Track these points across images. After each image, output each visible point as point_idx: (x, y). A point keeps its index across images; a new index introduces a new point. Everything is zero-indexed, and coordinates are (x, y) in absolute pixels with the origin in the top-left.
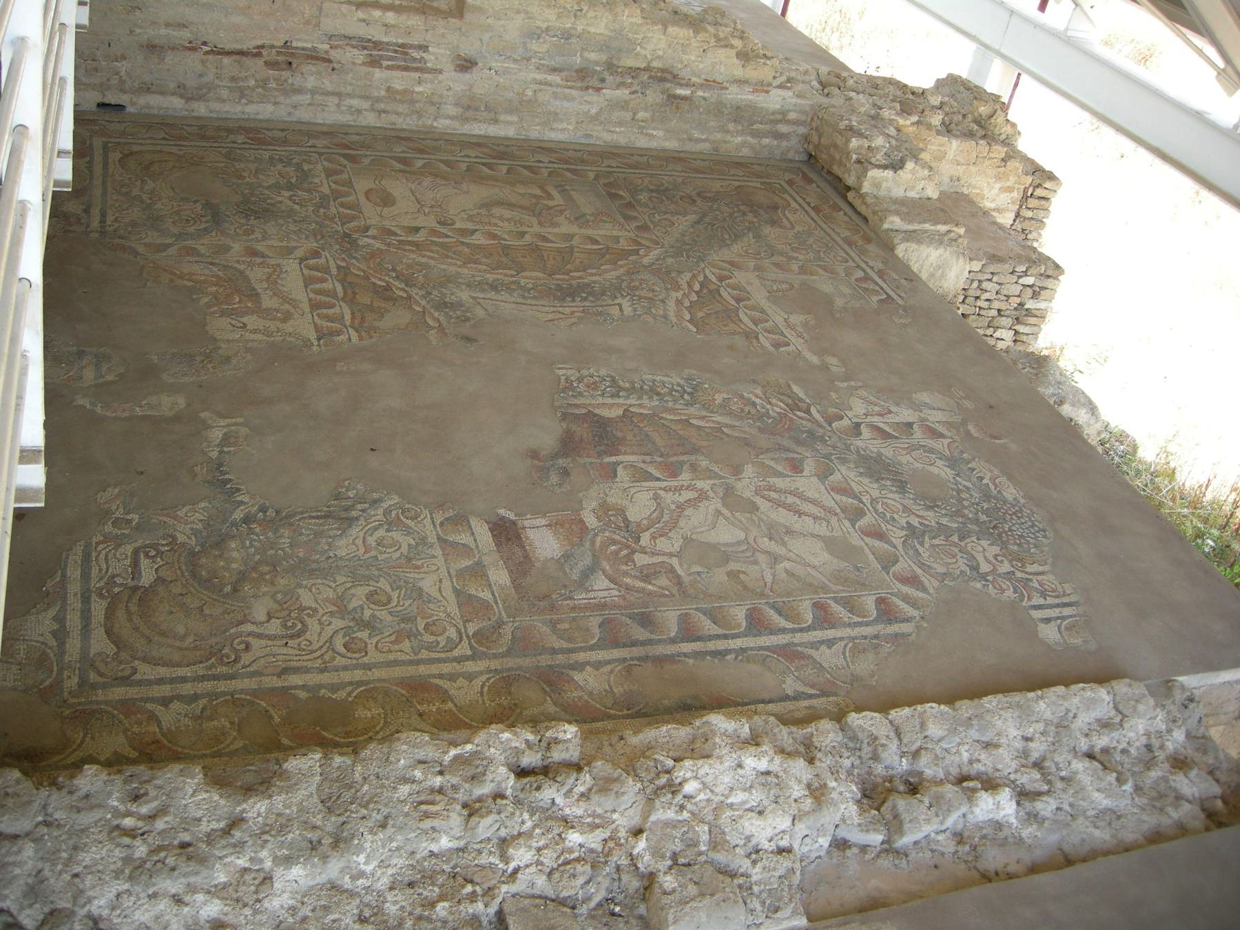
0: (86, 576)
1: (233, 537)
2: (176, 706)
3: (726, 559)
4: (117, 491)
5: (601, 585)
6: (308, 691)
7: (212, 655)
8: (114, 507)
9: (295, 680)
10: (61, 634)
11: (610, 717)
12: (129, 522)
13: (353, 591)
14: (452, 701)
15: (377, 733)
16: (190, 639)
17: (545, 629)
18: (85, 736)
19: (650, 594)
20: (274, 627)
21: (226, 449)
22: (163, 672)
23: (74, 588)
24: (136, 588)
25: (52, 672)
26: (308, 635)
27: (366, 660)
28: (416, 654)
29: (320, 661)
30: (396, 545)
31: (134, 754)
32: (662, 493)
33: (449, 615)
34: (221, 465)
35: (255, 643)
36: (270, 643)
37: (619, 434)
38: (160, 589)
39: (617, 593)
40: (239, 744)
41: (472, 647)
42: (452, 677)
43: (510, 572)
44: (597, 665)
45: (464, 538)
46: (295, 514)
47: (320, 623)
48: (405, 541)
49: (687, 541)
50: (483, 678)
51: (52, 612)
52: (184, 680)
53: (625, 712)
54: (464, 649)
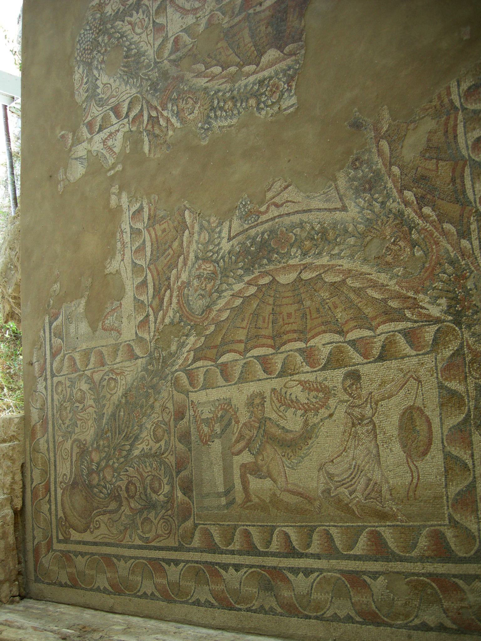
37: (270, 29)
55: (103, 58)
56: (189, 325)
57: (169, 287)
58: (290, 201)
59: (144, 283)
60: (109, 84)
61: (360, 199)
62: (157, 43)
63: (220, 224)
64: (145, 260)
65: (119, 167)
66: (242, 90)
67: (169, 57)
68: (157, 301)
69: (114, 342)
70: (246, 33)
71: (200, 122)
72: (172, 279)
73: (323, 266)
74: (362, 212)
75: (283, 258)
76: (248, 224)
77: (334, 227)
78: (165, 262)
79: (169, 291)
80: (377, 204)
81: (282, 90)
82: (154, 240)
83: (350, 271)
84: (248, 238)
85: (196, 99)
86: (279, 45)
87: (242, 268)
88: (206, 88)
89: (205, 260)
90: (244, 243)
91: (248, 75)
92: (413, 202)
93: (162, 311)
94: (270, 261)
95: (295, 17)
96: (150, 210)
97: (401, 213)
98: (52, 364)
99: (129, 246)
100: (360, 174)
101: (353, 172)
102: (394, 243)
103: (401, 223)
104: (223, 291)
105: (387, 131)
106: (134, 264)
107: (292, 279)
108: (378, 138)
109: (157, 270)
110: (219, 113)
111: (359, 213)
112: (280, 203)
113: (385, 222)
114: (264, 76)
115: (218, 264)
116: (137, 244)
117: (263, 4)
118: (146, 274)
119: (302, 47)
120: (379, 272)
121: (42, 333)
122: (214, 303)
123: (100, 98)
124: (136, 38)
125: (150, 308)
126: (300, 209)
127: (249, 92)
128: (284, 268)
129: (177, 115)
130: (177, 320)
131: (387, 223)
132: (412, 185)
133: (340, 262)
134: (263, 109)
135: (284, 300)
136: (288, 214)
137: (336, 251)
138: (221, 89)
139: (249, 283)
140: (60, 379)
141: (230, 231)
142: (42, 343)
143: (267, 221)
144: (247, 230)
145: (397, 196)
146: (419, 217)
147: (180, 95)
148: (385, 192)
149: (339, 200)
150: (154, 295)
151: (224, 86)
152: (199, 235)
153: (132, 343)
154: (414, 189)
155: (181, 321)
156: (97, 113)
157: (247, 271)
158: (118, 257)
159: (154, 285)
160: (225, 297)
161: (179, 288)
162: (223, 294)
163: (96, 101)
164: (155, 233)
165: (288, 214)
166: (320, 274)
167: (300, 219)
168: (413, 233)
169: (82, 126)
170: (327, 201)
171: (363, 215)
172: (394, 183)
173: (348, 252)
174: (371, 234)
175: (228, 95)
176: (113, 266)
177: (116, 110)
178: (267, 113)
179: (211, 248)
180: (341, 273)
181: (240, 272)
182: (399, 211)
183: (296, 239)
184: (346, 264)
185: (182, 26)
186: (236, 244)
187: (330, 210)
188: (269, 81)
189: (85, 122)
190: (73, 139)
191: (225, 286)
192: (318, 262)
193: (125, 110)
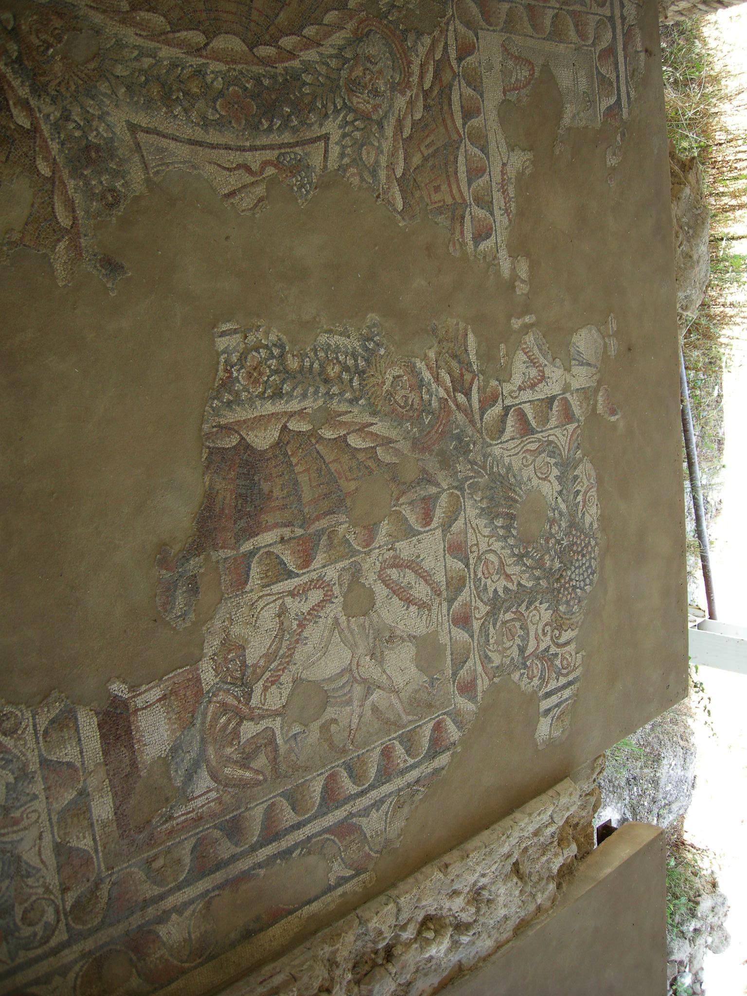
5: (204, 782)
11: (183, 972)
17: (140, 875)
32: (288, 600)
33: (47, 890)
37: (265, 487)
39: (213, 795)
43: (115, 795)
45: (68, 753)
53: (198, 961)
55: (551, 528)
56: (390, 22)
57: (426, 94)
58: (224, 168)
59: (468, 115)
60: (539, 478)
61: (105, 135)
62: (459, 524)
63: (343, 168)
64: (466, 151)
65: (516, 324)
66: (311, 390)
67: (439, 493)
68: (447, 76)
69: (512, 36)
70: (307, 495)
71: (382, 357)
72: (420, 104)
73: (168, 43)
74: (103, 113)
75: (236, 77)
76: (295, 154)
77: (150, 102)
78: (432, 137)
79: (427, 86)
80: (77, 119)
81: (241, 368)
82: (452, 179)
83: (123, 22)
84: (294, 130)
85: (390, 401)
86: (249, 452)
87: (305, 84)
88: (374, 414)
89: (366, 117)
90: (302, 123)
91: (301, 413)
92: (14, 104)
93: (437, 59)
94: (258, 80)
95: (220, 497)
96: (462, 233)
97: (38, 90)
98: (614, 38)
99: (494, 184)
100: (104, 178)
101: (118, 185)
102: (49, 46)
103: (35, 75)
104: (336, 56)
105: (59, 240)
106: (484, 149)
107: (221, 38)
108: (73, 232)
109: (446, 126)
110: (350, 362)
111: (108, 114)
112: (241, 171)
113: (63, 84)
114: (273, 404)
115: (345, 103)
116: (481, 181)
117: (278, 540)
118: (464, 128)
119: (208, 436)
120: (73, 5)
121: (633, 94)
122: (349, 43)
123: (554, 457)
124: (497, 546)
125: (456, 70)
126: (207, 150)
127: (299, 383)
128: (234, 62)
129: (421, 384)
130: (411, 37)
131: (60, 83)
132: (17, 136)
133: (140, 41)
134: (275, 345)
135: (234, 10)
136: (227, 148)
137: (147, 62)
138: (346, 404)
139: (292, 55)
140: (600, 11)
141: (326, 151)
142: (632, 78)
143: (264, 148)
144: (297, 144)
145: (42, 122)
146: (5, 77)
147: (418, 416)
148: (62, 136)
149: (141, 144)
150: (451, 90)
151: (343, 407)
152: (377, 162)
153: (483, 24)
154: (13, 127)
155: (405, 32)
156: (558, 432)
157: (295, 76)
158: (511, 172)
159: (450, 105)
160: (331, 46)
161: (408, 85)
162: (336, 52)
163: (560, 455)
164: (451, 191)
165: (227, 148)
166: (173, 32)
167: (208, 134)
168: (16, 54)
169: (582, 419)
170: (161, 150)
171: (100, 108)
172: (47, 147)
173: (125, 52)
174: (86, 71)
175: (335, 390)
176: (518, 161)
177: (526, 429)
178: (267, 334)
179: (357, 134)
180: (138, 24)
181: (308, 79)
182: (39, 96)
183: (215, 103)
184: (130, 36)
185: (419, 541)
186: (316, 126)
187: (158, 133)
188: (264, 392)
189: (576, 425)
190: (596, 401)
191: (333, 63)
192: (177, 53)
193: (510, 421)
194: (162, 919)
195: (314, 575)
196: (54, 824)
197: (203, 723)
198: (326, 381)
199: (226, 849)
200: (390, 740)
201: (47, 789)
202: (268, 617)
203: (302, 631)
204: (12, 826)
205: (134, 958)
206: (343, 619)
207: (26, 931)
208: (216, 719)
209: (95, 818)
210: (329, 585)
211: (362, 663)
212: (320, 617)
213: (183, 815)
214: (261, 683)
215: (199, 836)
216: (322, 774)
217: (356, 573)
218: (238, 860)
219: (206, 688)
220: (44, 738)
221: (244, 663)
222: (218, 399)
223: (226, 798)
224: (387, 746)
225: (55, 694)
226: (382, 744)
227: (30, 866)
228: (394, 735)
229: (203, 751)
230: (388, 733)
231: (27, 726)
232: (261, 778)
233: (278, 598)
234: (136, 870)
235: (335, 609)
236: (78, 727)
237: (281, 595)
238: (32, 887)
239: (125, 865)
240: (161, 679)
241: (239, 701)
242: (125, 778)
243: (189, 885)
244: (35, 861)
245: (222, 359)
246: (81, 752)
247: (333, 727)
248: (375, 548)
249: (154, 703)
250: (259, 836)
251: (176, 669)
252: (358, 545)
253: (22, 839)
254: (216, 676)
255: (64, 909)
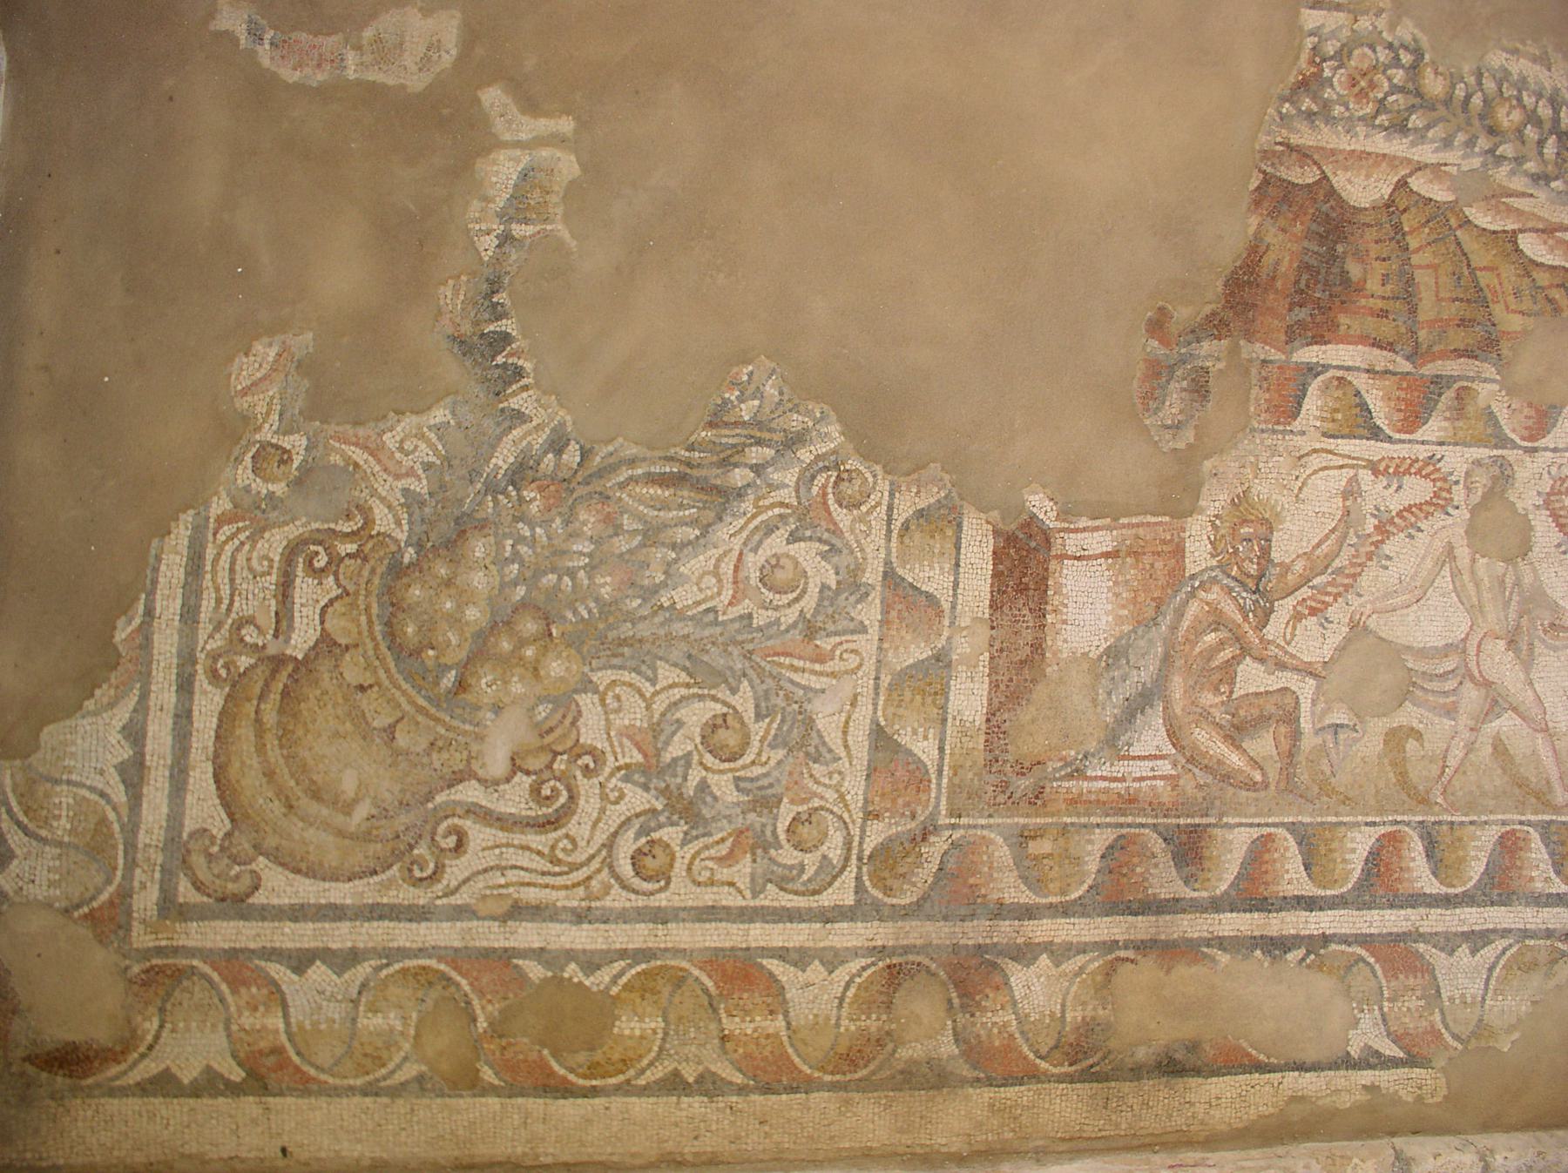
0: (189, 614)
1: (482, 526)
2: (319, 972)
3: (1405, 693)
4: (272, 353)
5: (1151, 736)
6: (548, 965)
7: (397, 855)
8: (261, 408)
9: (527, 935)
10: (134, 774)
11: (1034, 1076)
12: (285, 457)
13: (681, 713)
14: (786, 1014)
15: (643, 1071)
16: (362, 811)
17: (1003, 852)
18: (161, 1027)
19: (1227, 777)
20: (515, 799)
21: (518, 230)
22: (308, 891)
23: (166, 644)
24: (279, 661)
25: (115, 868)
26: (572, 827)
27: (661, 900)
28: (755, 895)
29: (581, 891)
30: (795, 586)
31: (237, 1075)
32: (1366, 476)
33: (842, 797)
34: (494, 286)
35: (480, 835)
36: (502, 836)
37: (1354, 270)
38: (324, 666)
39: (1165, 767)
40: (411, 1070)
41: (859, 888)
42: (799, 958)
43: (995, 686)
44: (1061, 952)
45: (932, 578)
46: (612, 469)
47: (604, 797)
48: (822, 574)
49: (1357, 628)
50: (855, 965)
51: (122, 714)
52: (336, 913)
53: (1066, 1069)
54: (842, 893)
81: (1340, 67)
86: (1332, 203)
91: (1437, 170)
114: (1388, 139)
134: (1406, 48)
138: (1525, 180)
151: (1518, 184)
175: (1506, 149)
178: (1392, 27)
194: (1024, 953)
195: (1423, 452)
196: (882, 691)
197: (1174, 628)
198: (1492, 131)
199: (1165, 881)
200: (1521, 823)
201: (885, 622)
202: (1326, 488)
203: (1382, 542)
204: (813, 661)
205: (956, 1001)
206: (1463, 553)
207: (788, 856)
208: (1197, 631)
209: (952, 708)
210: (1445, 480)
211: (1488, 646)
212: (1419, 530)
213: (1103, 778)
214: (1290, 602)
215: (1124, 831)
216: (1374, 824)
217: (1503, 476)
218: (1184, 911)
219: (1191, 568)
220: (901, 536)
221: (1265, 552)
222: (1292, 103)
223: (1188, 784)
224: (1513, 832)
225: (935, 468)
226: (1504, 823)
227: (824, 743)
228: (1533, 818)
229: (1162, 679)
230: (1521, 807)
231: (878, 504)
232: (1258, 778)
233: (1352, 467)
234: (1000, 840)
235: (1451, 526)
236: (959, 539)
237: (1352, 463)
238: (817, 782)
239: (983, 821)
240: (1116, 519)
241: (1246, 618)
242: (1020, 669)
243: (1083, 915)
244: (833, 739)
245: (1309, 42)
246: (956, 585)
247: (1411, 745)
248: (1546, 449)
249: (1096, 557)
250: (1232, 884)
251: (1145, 513)
252: (1514, 431)
253: (823, 691)
254: (1213, 556)
255: (861, 851)
